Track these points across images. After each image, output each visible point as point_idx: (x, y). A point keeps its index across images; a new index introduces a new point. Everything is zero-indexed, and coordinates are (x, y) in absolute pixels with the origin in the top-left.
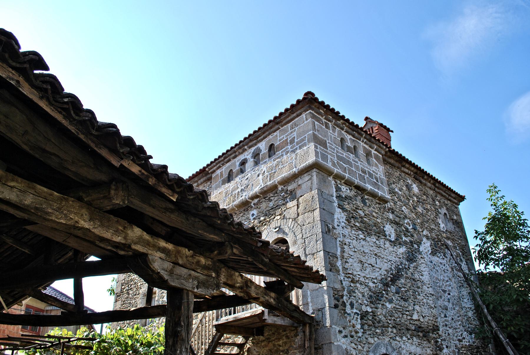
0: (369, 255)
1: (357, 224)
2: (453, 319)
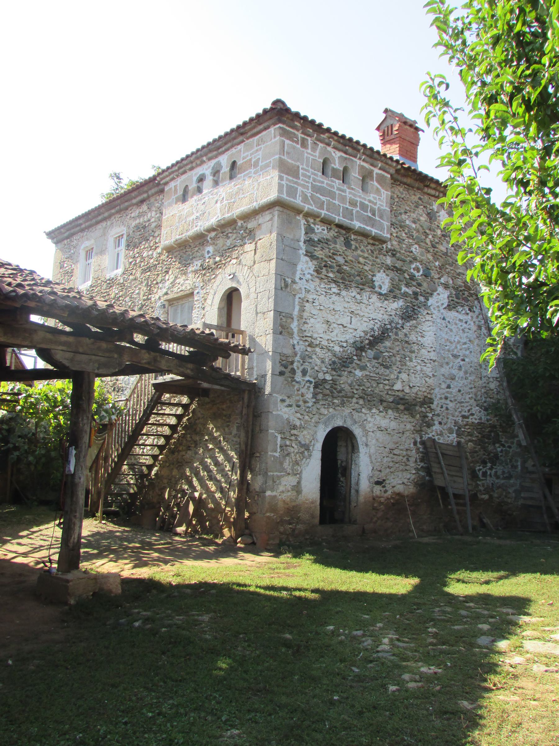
1: (331, 275)
2: (459, 391)
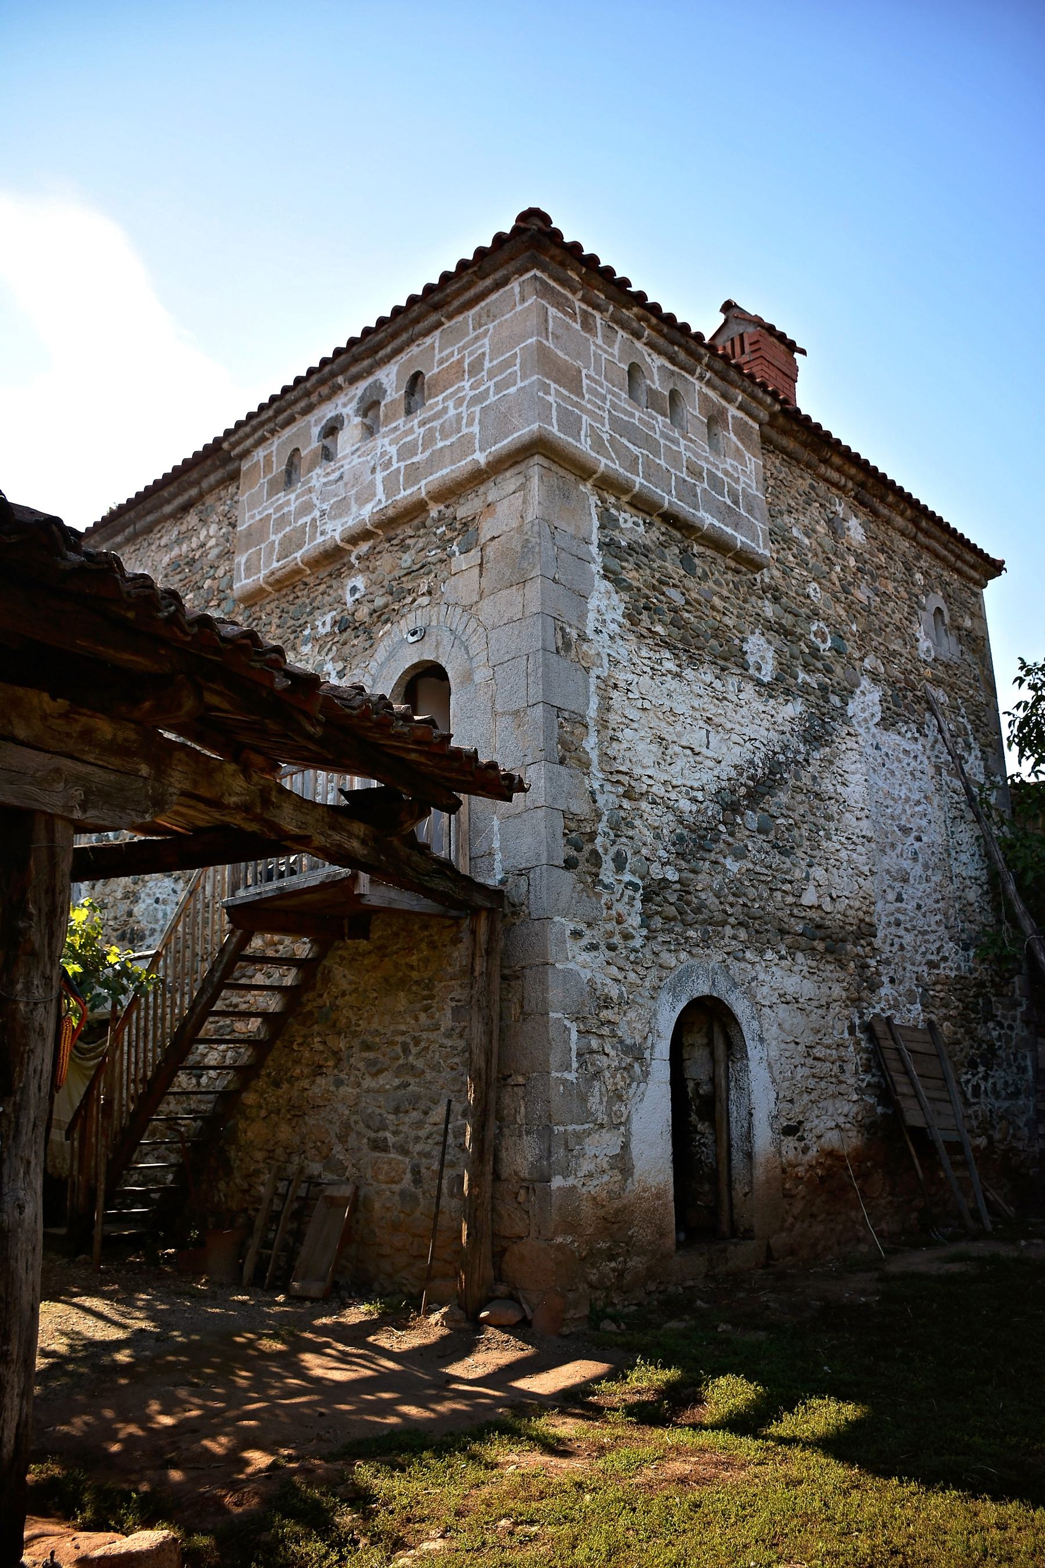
0: (689, 721)
1: (659, 629)
2: (919, 907)
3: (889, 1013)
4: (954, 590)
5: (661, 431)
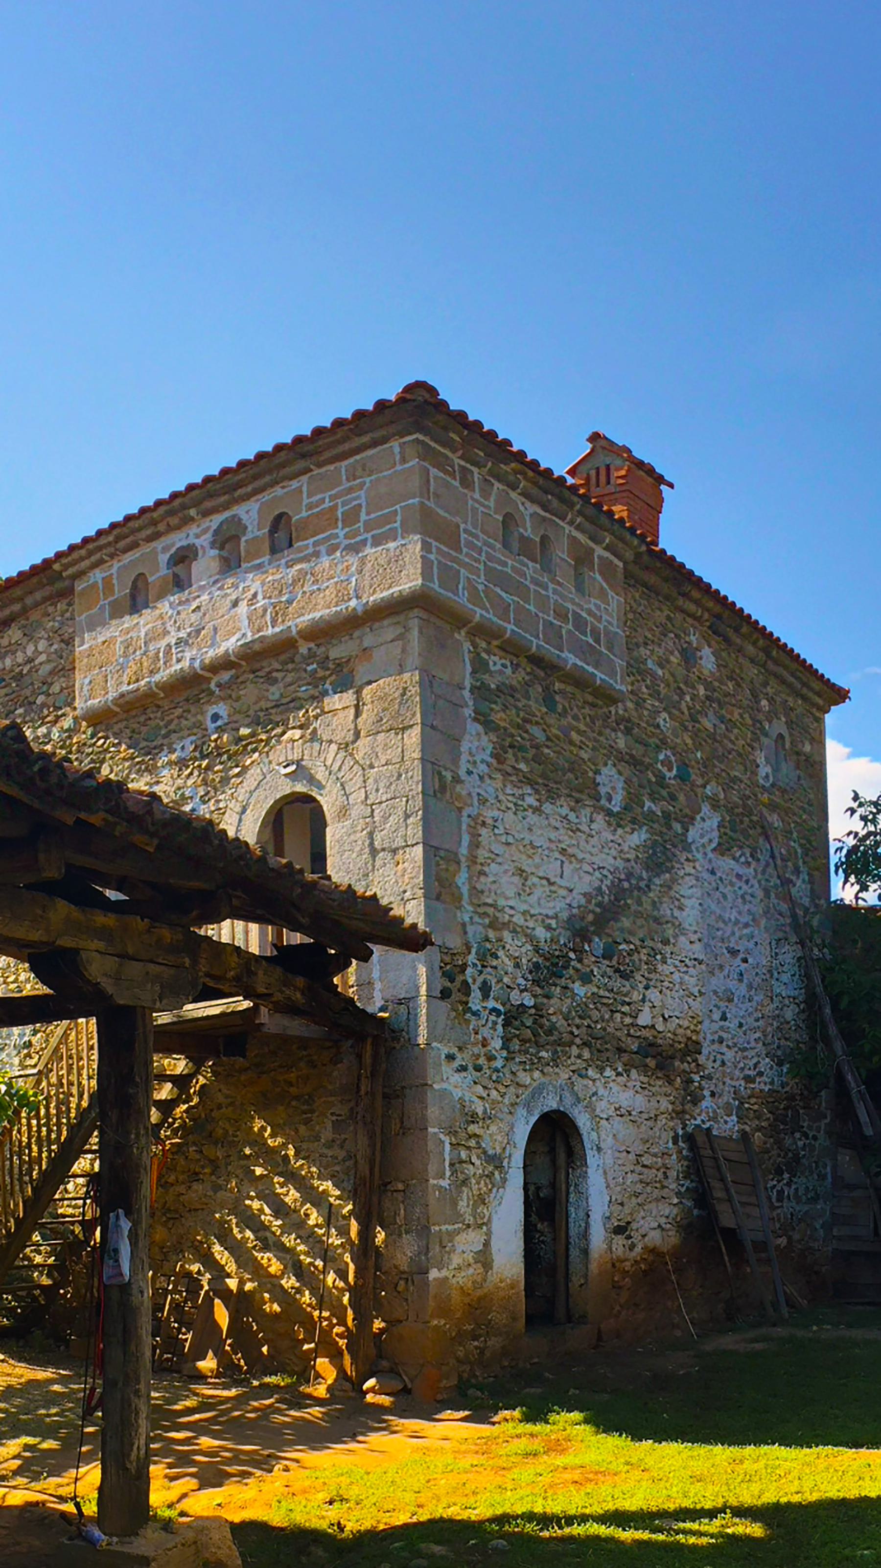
0: (546, 852)
1: (522, 766)
2: (741, 1025)
3: (707, 1125)
4: (797, 716)
5: (531, 577)
